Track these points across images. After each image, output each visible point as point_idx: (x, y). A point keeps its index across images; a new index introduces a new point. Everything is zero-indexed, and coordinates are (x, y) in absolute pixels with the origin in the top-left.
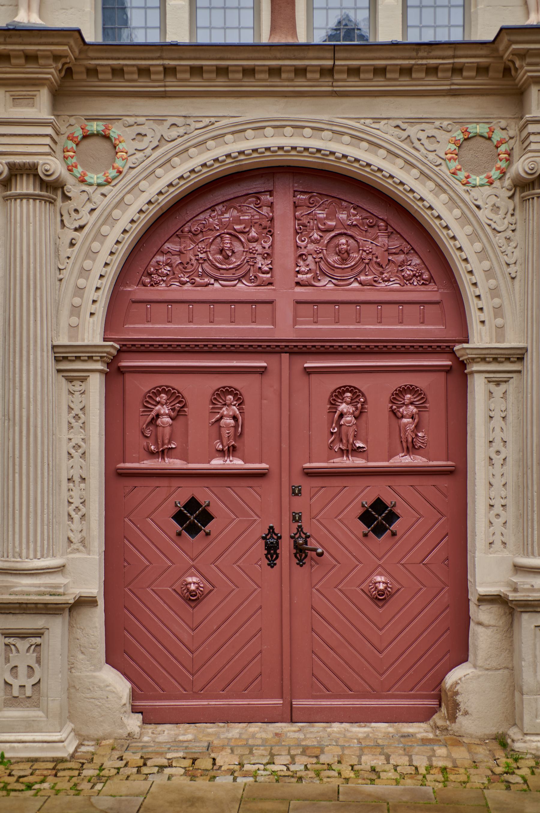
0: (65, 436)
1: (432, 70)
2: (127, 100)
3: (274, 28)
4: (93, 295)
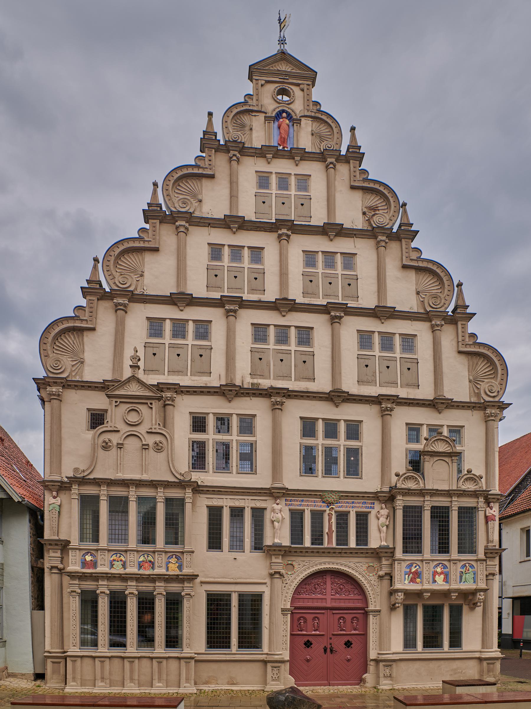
1: (362, 553)
2: (296, 557)
3: (328, 543)
4: (289, 598)
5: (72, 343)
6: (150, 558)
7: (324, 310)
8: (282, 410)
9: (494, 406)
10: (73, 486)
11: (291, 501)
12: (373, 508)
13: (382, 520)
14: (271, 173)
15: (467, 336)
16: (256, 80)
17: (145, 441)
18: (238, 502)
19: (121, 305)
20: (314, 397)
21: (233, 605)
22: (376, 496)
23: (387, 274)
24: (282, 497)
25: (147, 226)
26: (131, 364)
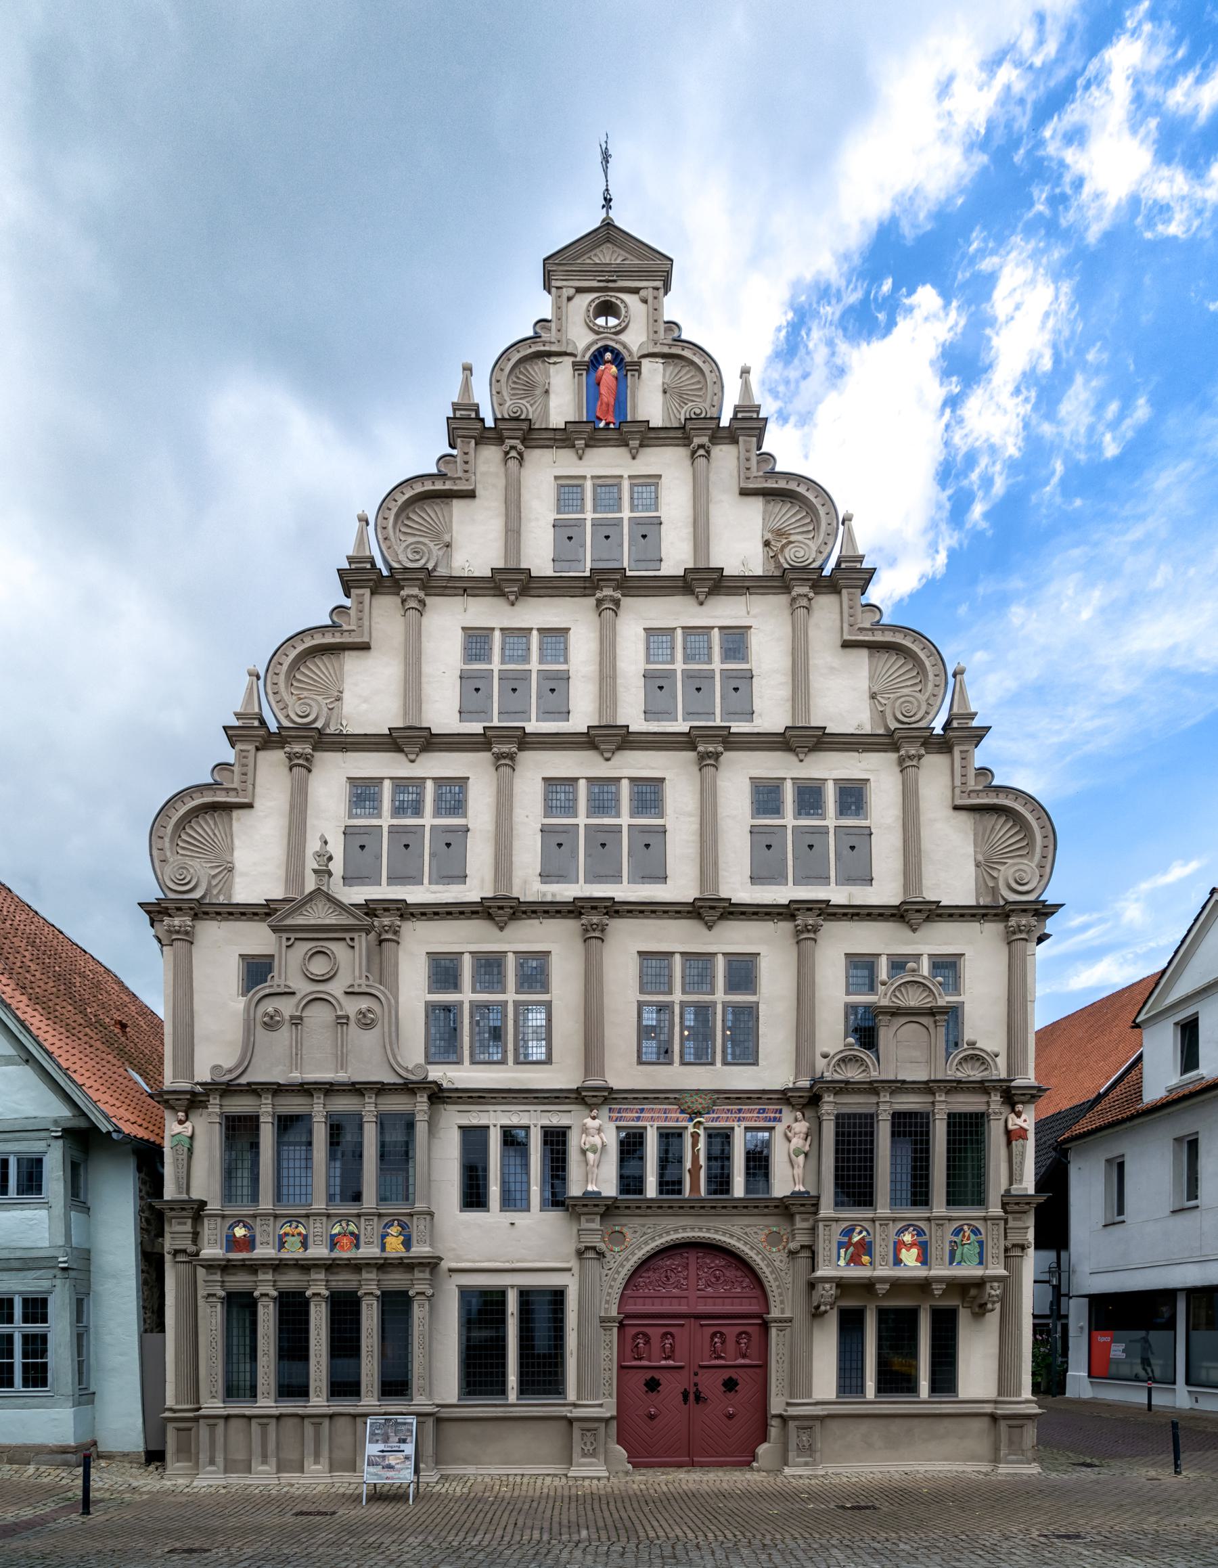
0: (603, 1352)
5: (211, 834)
6: (352, 1227)
7: (687, 741)
8: (603, 941)
9: (1024, 911)
10: (211, 1099)
11: (619, 1111)
12: (780, 1120)
13: (797, 1142)
14: (584, 477)
15: (971, 773)
16: (558, 288)
17: (341, 1010)
18: (514, 1116)
19: (298, 758)
20: (665, 912)
21: (510, 1313)
22: (785, 1097)
23: (811, 663)
24: (603, 1103)
25: (347, 602)
26: (316, 867)
